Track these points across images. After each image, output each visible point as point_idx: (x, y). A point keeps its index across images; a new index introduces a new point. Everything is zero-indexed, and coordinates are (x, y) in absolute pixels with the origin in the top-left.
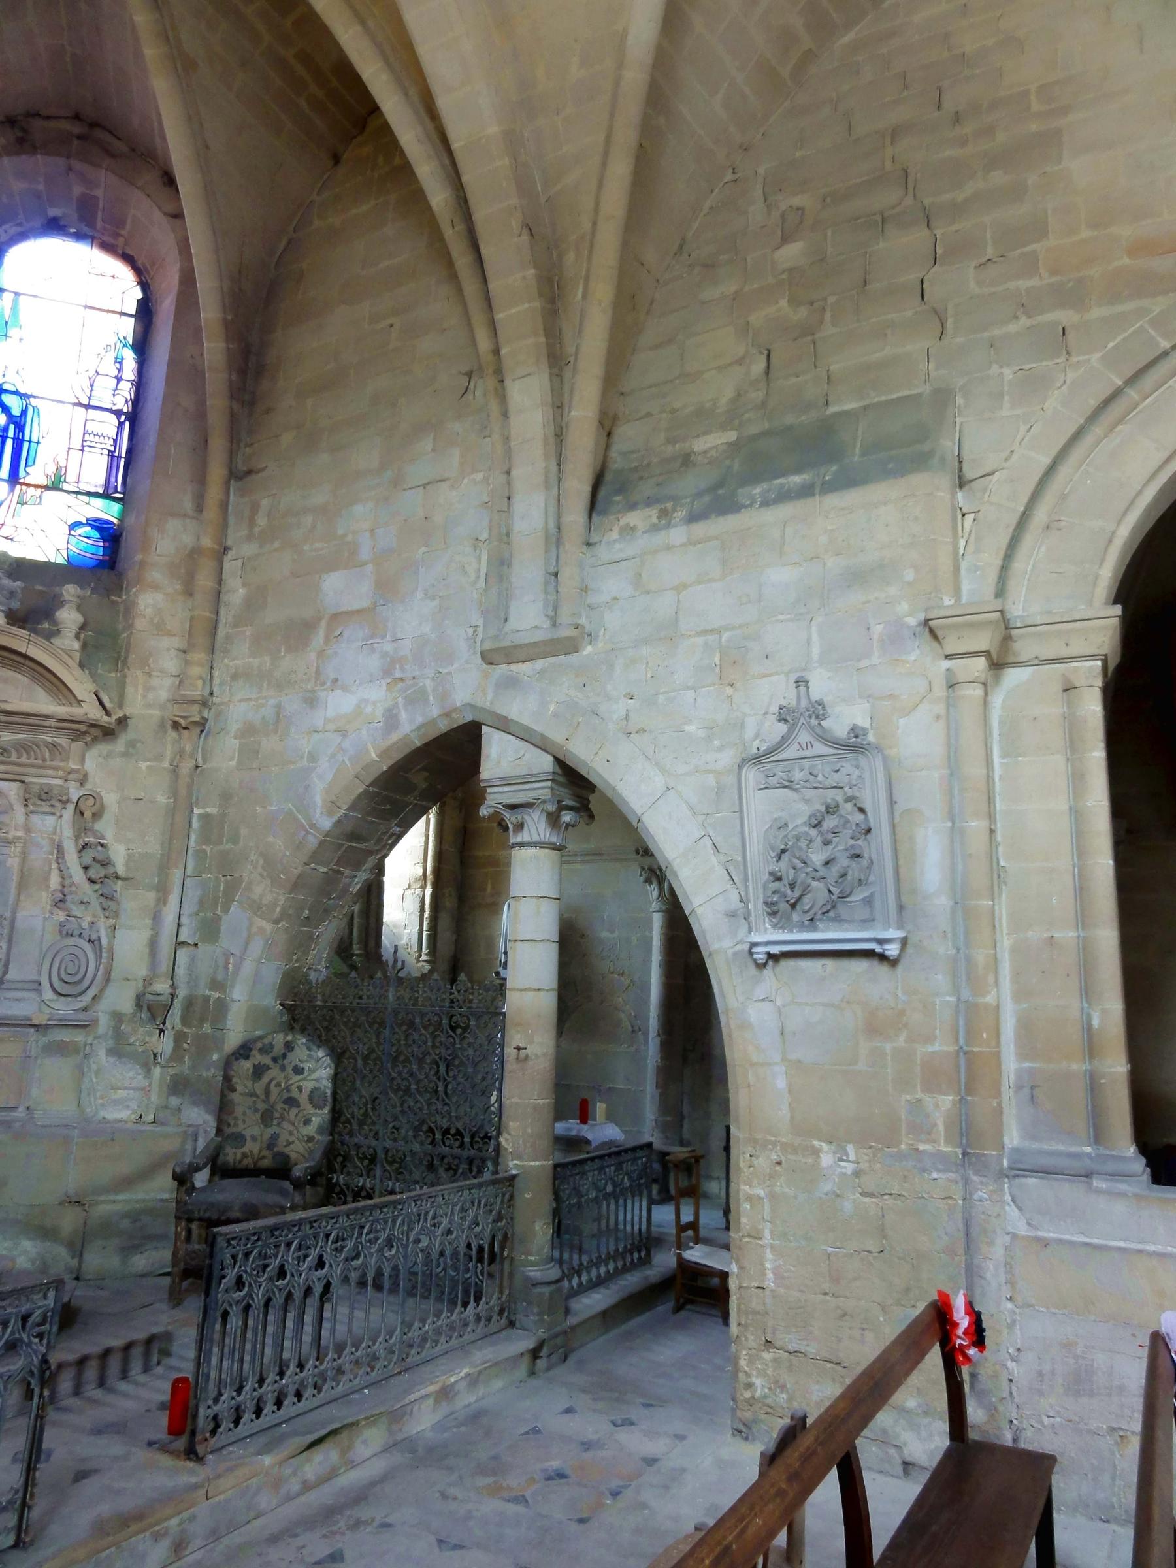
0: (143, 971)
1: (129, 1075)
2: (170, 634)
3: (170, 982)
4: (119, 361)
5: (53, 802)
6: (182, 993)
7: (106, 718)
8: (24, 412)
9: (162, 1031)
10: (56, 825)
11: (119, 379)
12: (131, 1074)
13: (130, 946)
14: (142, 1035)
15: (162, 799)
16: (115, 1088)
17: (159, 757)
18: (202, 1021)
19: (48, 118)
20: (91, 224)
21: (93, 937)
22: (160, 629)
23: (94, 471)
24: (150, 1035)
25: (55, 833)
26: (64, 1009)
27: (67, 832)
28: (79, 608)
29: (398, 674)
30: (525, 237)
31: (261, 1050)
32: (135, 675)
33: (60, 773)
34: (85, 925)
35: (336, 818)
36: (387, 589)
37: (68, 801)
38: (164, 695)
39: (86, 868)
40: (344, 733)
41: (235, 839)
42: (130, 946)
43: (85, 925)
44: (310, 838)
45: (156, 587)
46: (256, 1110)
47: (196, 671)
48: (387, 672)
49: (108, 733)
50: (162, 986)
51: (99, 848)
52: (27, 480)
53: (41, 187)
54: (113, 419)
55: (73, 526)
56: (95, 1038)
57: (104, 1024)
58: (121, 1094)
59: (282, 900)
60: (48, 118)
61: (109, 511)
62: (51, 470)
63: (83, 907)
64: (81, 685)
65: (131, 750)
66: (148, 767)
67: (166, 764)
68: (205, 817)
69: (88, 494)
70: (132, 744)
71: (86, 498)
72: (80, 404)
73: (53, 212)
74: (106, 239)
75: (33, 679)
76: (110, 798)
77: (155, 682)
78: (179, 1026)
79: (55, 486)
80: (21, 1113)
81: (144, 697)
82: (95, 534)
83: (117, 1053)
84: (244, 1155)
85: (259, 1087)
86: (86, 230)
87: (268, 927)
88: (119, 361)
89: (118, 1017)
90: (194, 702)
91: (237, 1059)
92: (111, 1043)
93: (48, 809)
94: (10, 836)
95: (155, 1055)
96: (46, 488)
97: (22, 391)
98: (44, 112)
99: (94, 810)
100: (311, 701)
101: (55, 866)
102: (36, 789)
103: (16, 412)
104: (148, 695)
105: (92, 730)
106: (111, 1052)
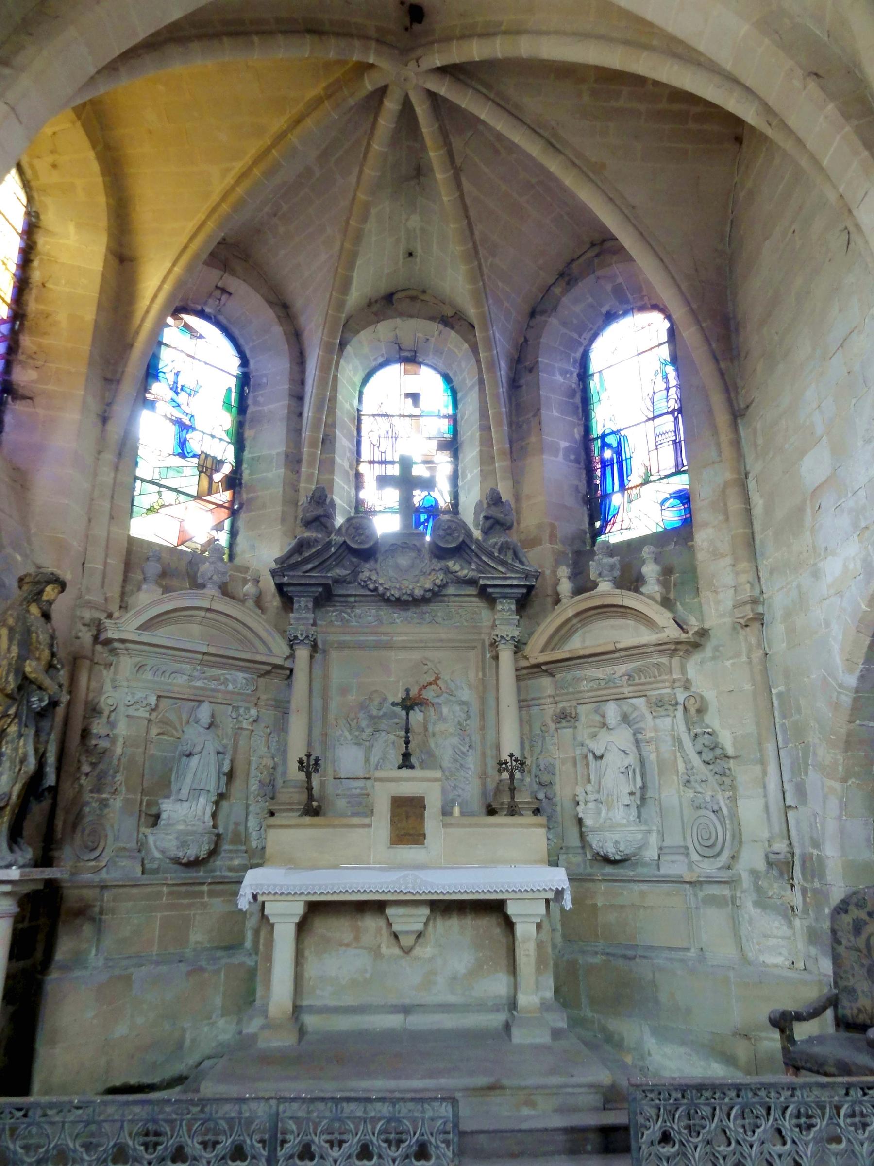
0: (766, 835)
1: (775, 925)
2: (723, 556)
3: (787, 842)
4: (666, 378)
5: (667, 707)
6: (797, 851)
7: (684, 635)
8: (619, 443)
9: (792, 886)
11: (668, 389)
12: (777, 924)
13: (753, 812)
14: (775, 888)
15: (748, 687)
16: (766, 936)
17: (738, 655)
18: (813, 877)
19: (579, 258)
20: (627, 302)
21: (716, 808)
22: (716, 554)
23: (667, 459)
24: (785, 890)
25: (673, 729)
26: (709, 868)
27: (682, 727)
28: (656, 561)
29: (863, 525)
30: (812, 84)
31: (857, 905)
32: (705, 594)
33: (667, 684)
34: (708, 799)
35: (857, 673)
36: (840, 451)
37: (677, 704)
38: (730, 604)
39: (700, 753)
40: (839, 593)
41: (799, 711)
42: (753, 812)
43: (708, 799)
44: (843, 697)
45: (706, 525)
46: (863, 965)
47: (743, 578)
48: (855, 525)
49: (695, 646)
50: (780, 846)
51: (706, 736)
52: (630, 486)
53: (590, 300)
54: (670, 418)
55: (662, 504)
56: (742, 892)
57: (746, 881)
58: (772, 942)
59: (840, 759)
60: (579, 258)
61: (681, 482)
62: (642, 471)
63: (703, 784)
64: (662, 617)
65: (717, 654)
66: (733, 664)
67: (744, 659)
68: (780, 695)
69: (667, 476)
70: (716, 649)
71: (665, 480)
72: (649, 419)
73: (604, 310)
74: (639, 304)
75: (635, 620)
76: (710, 695)
77: (721, 596)
78: (802, 882)
79: (647, 482)
80: (692, 953)
81: (717, 610)
82: (677, 502)
83: (762, 903)
84: (860, 1011)
85: (861, 942)
86: (626, 306)
87: (837, 785)
88: (666, 378)
89: (754, 873)
90: (745, 603)
91: (838, 913)
92: (754, 896)
93: (664, 713)
94: (647, 737)
95: (792, 908)
96: (642, 485)
97: (615, 430)
98: (576, 256)
99: (697, 706)
100: (816, 575)
101: (678, 754)
102: (653, 699)
103: (615, 445)
104: (716, 608)
105: (679, 646)
106: (756, 904)
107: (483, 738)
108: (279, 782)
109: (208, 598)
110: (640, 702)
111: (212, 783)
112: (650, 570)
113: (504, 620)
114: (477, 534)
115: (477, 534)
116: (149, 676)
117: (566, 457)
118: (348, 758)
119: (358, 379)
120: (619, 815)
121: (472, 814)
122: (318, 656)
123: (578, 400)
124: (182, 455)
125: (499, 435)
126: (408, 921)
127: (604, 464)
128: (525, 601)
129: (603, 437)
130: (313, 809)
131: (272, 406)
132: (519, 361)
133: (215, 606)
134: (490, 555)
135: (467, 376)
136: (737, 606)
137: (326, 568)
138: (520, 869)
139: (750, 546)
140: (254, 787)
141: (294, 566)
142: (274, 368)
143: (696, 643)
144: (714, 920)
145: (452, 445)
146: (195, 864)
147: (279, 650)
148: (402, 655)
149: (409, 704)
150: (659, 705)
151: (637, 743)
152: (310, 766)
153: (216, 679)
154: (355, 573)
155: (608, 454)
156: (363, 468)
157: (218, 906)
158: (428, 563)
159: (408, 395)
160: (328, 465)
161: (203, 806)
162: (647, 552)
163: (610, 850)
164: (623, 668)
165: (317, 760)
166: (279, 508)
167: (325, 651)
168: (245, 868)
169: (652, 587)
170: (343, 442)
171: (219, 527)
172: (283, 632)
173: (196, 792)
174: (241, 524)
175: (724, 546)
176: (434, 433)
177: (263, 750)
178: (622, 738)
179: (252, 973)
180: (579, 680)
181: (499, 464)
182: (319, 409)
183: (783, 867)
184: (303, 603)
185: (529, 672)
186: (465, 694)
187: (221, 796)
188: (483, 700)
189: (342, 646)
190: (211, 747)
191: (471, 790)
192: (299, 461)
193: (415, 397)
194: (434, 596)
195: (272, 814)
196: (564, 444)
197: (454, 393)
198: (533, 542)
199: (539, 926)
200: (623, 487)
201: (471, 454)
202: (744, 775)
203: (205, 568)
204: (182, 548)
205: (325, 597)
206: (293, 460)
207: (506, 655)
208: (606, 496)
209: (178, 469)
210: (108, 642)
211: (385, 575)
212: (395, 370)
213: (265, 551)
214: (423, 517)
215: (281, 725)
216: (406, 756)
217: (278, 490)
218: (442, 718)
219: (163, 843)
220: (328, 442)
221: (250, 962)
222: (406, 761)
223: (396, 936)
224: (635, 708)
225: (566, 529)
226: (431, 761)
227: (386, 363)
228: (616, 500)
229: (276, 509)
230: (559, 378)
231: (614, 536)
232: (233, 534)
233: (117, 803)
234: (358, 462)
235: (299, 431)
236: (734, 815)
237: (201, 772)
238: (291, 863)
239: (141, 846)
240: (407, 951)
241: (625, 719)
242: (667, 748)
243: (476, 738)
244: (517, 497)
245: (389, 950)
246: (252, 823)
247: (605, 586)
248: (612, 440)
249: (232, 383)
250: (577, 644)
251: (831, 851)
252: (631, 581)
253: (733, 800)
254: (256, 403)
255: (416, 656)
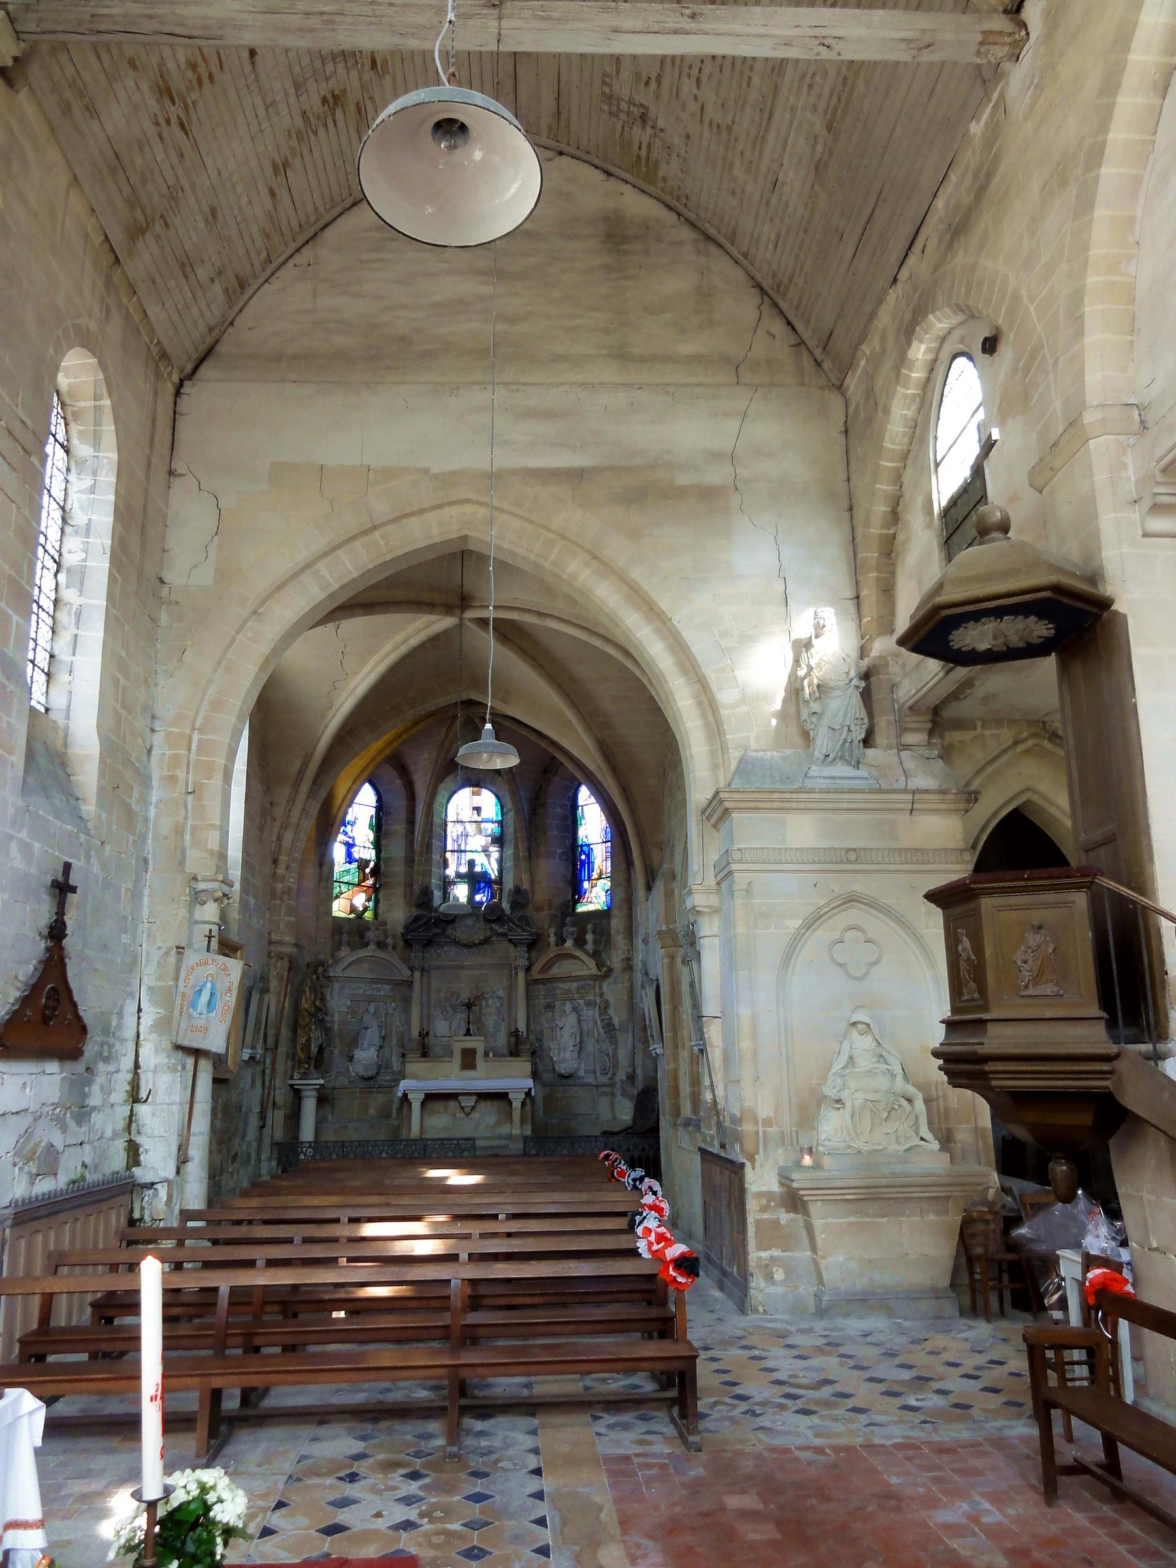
10: (590, 1014)
13: (623, 1055)
22: (618, 932)
23: (607, 867)
26: (604, 1080)
28: (594, 932)
42: (623, 1055)
57: (618, 1085)
64: (591, 963)
76: (611, 1000)
79: (600, 878)
89: (622, 1081)
104: (616, 960)
106: (623, 1095)
107: (509, 1016)
108: (406, 1039)
109: (371, 950)
110: (581, 1002)
111: (377, 1041)
112: (589, 937)
113: (519, 957)
114: (508, 911)
115: (508, 911)
116: (346, 991)
117: (561, 859)
118: (441, 1027)
119: (444, 802)
120: (568, 1055)
121: (502, 1056)
122: (425, 974)
123: (569, 822)
124: (350, 863)
125: (522, 847)
126: (469, 1102)
127: (583, 863)
128: (534, 944)
129: (582, 846)
130: (425, 1053)
131: (397, 827)
132: (537, 798)
133: (376, 954)
134: (514, 923)
135: (509, 805)
136: (623, 960)
137: (428, 927)
138: (516, 1079)
139: (630, 931)
140: (394, 1041)
141: (414, 930)
142: (398, 802)
143: (607, 974)
144: (604, 1102)
145: (499, 840)
146: (370, 1079)
147: (406, 972)
148: (469, 973)
149: (469, 1006)
150: (589, 1004)
151: (579, 1022)
152: (424, 1035)
153: (376, 989)
154: (444, 930)
155: (583, 857)
156: (448, 855)
157: (381, 1098)
158: (481, 924)
159: (474, 809)
160: (429, 860)
161: (373, 1052)
162: (589, 927)
163: (563, 1071)
164: (575, 984)
165: (427, 1033)
166: (402, 890)
167: (428, 971)
168: (397, 1081)
169: (590, 947)
170: (436, 843)
171: (369, 900)
172: (405, 960)
173: (370, 1046)
174: (381, 896)
175: (621, 929)
176: (489, 832)
177: (398, 1023)
178: (572, 1019)
179: (398, 1129)
180: (556, 989)
181: (524, 864)
182: (424, 836)
183: (631, 1078)
184: (417, 947)
185: (530, 984)
186: (501, 993)
187: (381, 1047)
188: (510, 997)
189: (438, 967)
190: (375, 1025)
191: (502, 1040)
192: (413, 861)
193: (478, 810)
194: (486, 941)
195: (403, 1055)
196: (560, 851)
197: (502, 807)
198: (539, 909)
199: (523, 1104)
200: (589, 879)
201: (509, 852)
202: (621, 1037)
203: (370, 935)
204: (352, 916)
205: (429, 943)
206: (410, 861)
207: (521, 975)
208: (581, 882)
209: (348, 871)
210: (329, 978)
211: (460, 932)
212: (465, 793)
213: (398, 915)
214: (482, 885)
215: (407, 1010)
216: (468, 1030)
217: (401, 879)
218: (487, 1005)
219: (357, 1069)
220: (429, 846)
221: (396, 1123)
222: (468, 1033)
223: (462, 1108)
224: (579, 1004)
225: (557, 902)
226: (481, 1030)
227: (462, 786)
228: (586, 885)
229: (400, 891)
230: (559, 810)
231: (581, 909)
232: (377, 902)
233: (336, 1051)
234: (445, 851)
235: (412, 842)
236: (615, 1057)
237: (372, 1035)
238: (415, 1077)
239: (348, 1070)
240: (468, 1115)
241: (575, 1009)
242: (591, 1025)
243: (506, 1015)
244: (532, 882)
245: (460, 1115)
246: (394, 1059)
247: (569, 943)
248: (585, 849)
249: (373, 812)
250: (555, 971)
251: (639, 1072)
252: (580, 942)
253: (615, 1050)
254: (387, 824)
255: (476, 973)
